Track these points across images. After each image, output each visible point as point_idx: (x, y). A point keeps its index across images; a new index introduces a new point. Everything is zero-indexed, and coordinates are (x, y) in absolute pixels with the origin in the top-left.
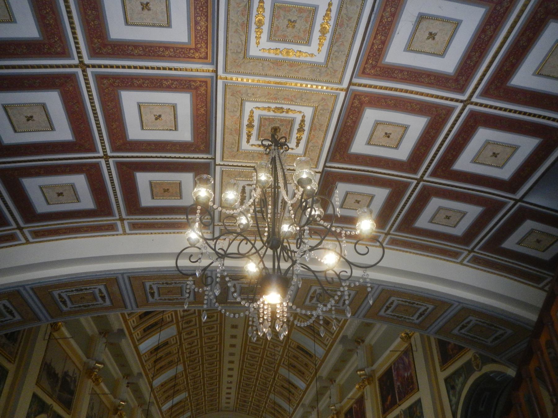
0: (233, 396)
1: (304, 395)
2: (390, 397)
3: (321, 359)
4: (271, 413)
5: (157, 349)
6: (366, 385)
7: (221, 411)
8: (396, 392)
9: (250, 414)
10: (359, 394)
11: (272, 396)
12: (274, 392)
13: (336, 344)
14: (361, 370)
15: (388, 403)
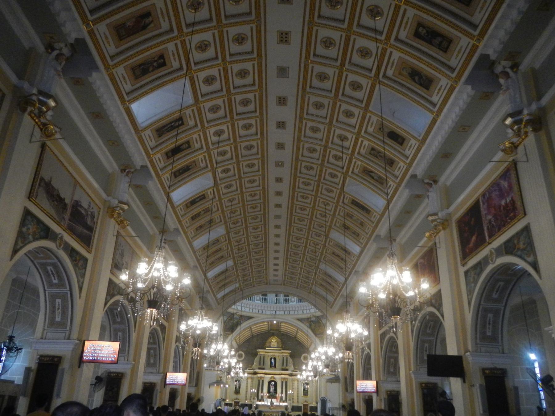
0: (280, 268)
1: (358, 260)
2: (474, 238)
3: (380, 213)
4: (321, 285)
5: (193, 202)
6: (440, 231)
7: (269, 284)
8: (485, 228)
9: (299, 287)
10: (431, 244)
11: (322, 266)
12: (325, 262)
13: (400, 189)
14: (431, 215)
15: (471, 245)
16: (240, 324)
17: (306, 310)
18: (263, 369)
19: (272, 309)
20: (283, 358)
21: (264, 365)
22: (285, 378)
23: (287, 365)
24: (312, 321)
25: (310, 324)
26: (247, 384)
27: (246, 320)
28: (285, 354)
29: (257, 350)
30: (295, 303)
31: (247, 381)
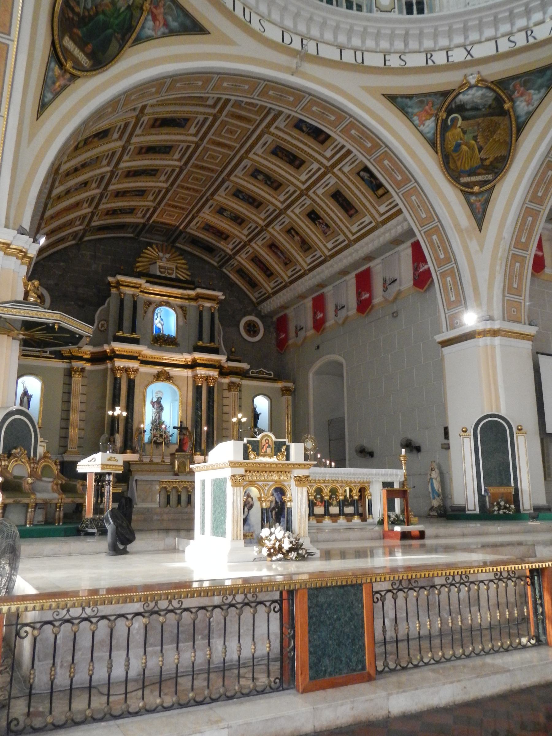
16: (138, 40)
17: (448, 50)
18: (136, 341)
19: (289, 23)
20: (201, 313)
21: (133, 330)
22: (207, 378)
23: (212, 340)
24: (461, 108)
25: (445, 121)
26: (68, 393)
27: (172, 33)
28: (208, 304)
29: (110, 279)
30: (395, 15)
31: (68, 384)
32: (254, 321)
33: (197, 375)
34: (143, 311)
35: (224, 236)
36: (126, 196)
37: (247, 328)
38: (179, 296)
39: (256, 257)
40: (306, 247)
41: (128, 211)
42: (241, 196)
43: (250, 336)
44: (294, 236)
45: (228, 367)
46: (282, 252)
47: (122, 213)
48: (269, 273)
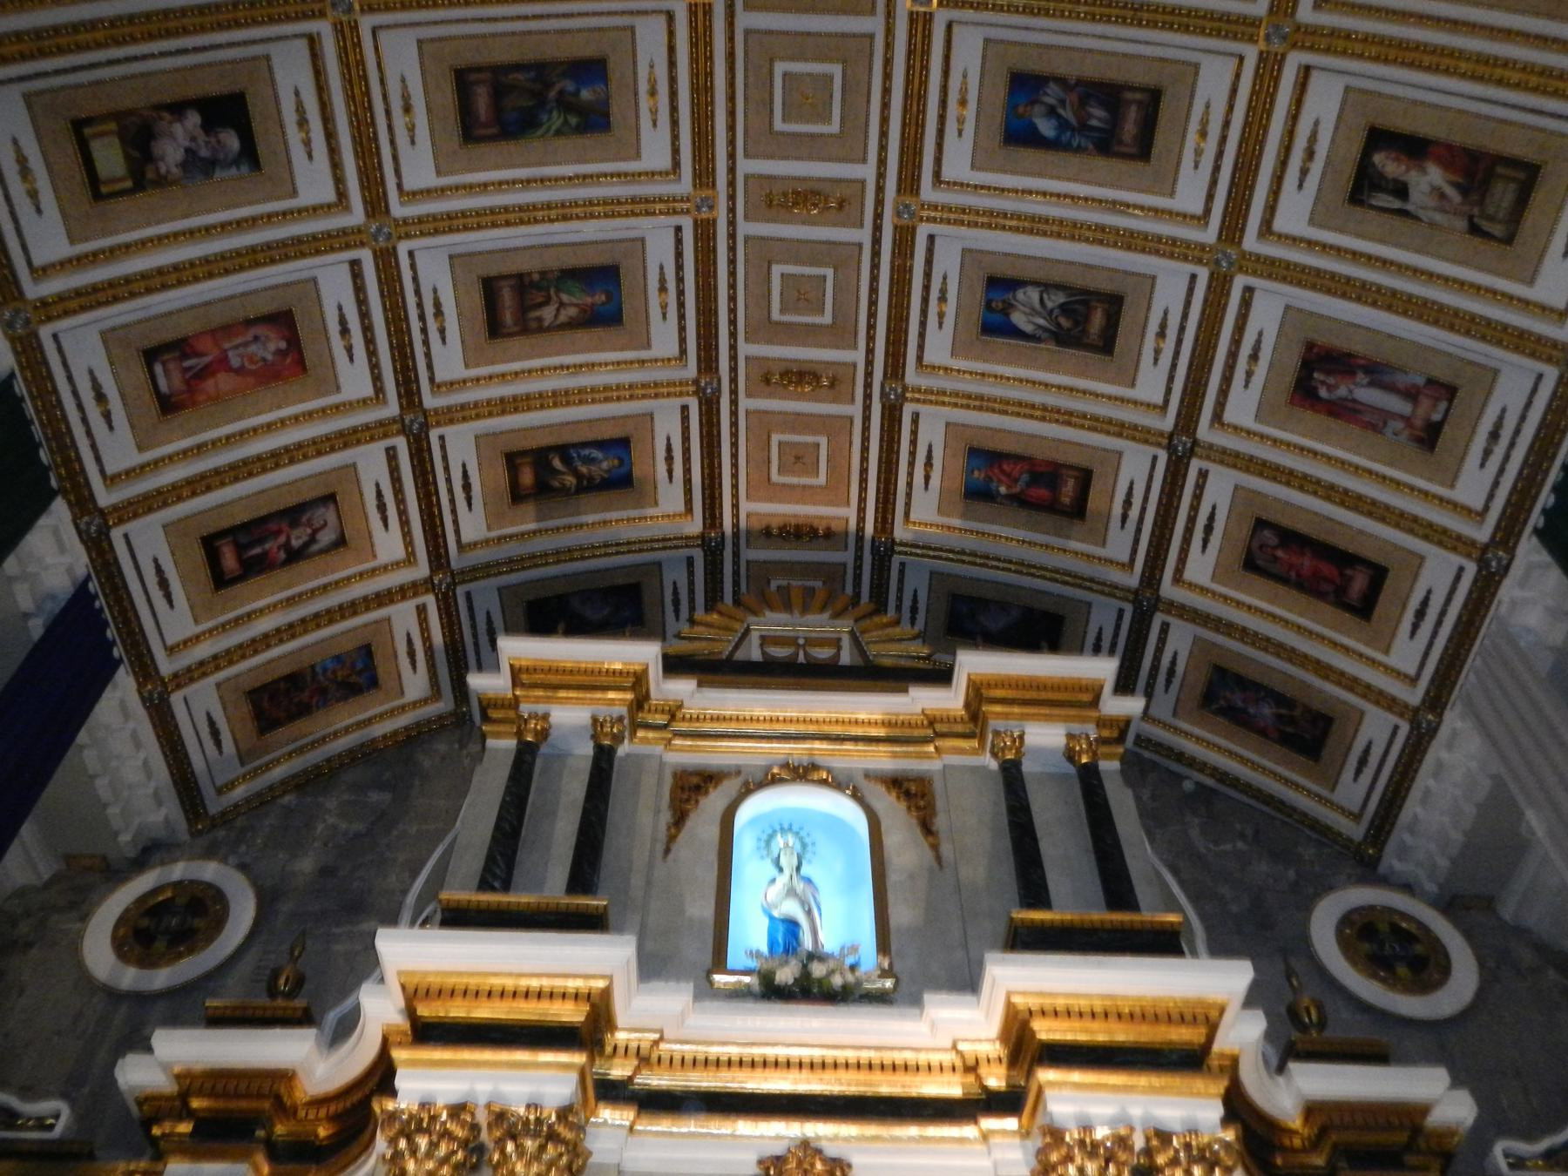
32: (1391, 910)
33: (1055, 1134)
34: (666, 817)
35: (1068, 489)
36: (541, 329)
37: (1366, 947)
38: (880, 732)
39: (1261, 524)
40: (1502, 195)
41: (606, 464)
42: (1046, 128)
43: (1392, 982)
44: (1401, 191)
45: (1312, 1110)
46: (1377, 372)
47: (589, 486)
48: (1359, 582)
